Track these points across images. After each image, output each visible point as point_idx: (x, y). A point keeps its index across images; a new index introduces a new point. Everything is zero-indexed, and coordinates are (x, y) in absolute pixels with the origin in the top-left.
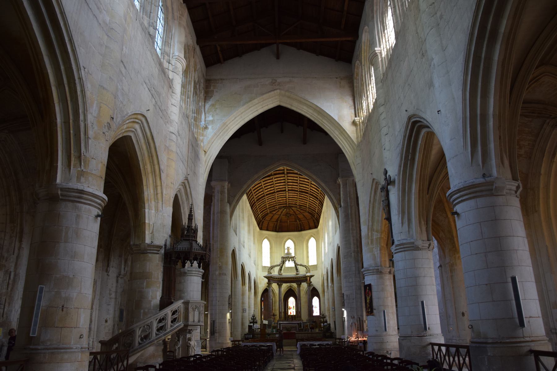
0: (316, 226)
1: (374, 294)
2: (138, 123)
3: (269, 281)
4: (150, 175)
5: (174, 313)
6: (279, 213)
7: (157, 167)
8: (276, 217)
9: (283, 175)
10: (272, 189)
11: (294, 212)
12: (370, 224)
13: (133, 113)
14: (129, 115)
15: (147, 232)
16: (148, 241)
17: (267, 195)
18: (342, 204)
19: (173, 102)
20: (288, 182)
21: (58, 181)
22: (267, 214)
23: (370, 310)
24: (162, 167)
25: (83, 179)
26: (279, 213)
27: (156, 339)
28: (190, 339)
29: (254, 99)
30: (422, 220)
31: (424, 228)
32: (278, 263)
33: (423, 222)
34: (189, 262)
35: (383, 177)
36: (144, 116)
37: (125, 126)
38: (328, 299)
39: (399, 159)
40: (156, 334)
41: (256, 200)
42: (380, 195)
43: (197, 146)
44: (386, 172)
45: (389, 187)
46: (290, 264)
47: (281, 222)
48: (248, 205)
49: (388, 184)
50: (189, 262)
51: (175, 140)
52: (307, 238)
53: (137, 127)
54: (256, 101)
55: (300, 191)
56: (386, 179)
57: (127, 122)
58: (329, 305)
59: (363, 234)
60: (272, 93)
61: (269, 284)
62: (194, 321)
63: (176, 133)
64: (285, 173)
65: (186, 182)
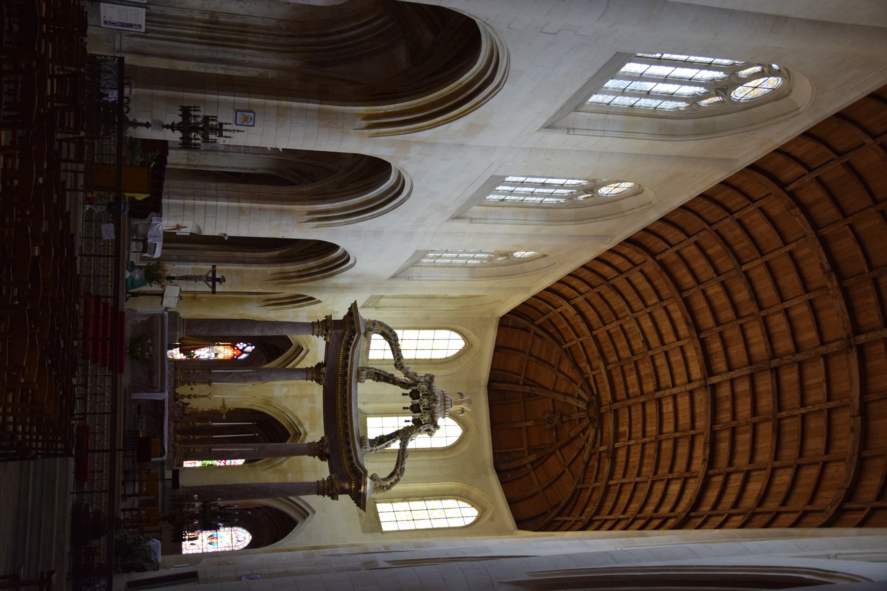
8: (546, 377)
11: (572, 440)
52: (475, 492)
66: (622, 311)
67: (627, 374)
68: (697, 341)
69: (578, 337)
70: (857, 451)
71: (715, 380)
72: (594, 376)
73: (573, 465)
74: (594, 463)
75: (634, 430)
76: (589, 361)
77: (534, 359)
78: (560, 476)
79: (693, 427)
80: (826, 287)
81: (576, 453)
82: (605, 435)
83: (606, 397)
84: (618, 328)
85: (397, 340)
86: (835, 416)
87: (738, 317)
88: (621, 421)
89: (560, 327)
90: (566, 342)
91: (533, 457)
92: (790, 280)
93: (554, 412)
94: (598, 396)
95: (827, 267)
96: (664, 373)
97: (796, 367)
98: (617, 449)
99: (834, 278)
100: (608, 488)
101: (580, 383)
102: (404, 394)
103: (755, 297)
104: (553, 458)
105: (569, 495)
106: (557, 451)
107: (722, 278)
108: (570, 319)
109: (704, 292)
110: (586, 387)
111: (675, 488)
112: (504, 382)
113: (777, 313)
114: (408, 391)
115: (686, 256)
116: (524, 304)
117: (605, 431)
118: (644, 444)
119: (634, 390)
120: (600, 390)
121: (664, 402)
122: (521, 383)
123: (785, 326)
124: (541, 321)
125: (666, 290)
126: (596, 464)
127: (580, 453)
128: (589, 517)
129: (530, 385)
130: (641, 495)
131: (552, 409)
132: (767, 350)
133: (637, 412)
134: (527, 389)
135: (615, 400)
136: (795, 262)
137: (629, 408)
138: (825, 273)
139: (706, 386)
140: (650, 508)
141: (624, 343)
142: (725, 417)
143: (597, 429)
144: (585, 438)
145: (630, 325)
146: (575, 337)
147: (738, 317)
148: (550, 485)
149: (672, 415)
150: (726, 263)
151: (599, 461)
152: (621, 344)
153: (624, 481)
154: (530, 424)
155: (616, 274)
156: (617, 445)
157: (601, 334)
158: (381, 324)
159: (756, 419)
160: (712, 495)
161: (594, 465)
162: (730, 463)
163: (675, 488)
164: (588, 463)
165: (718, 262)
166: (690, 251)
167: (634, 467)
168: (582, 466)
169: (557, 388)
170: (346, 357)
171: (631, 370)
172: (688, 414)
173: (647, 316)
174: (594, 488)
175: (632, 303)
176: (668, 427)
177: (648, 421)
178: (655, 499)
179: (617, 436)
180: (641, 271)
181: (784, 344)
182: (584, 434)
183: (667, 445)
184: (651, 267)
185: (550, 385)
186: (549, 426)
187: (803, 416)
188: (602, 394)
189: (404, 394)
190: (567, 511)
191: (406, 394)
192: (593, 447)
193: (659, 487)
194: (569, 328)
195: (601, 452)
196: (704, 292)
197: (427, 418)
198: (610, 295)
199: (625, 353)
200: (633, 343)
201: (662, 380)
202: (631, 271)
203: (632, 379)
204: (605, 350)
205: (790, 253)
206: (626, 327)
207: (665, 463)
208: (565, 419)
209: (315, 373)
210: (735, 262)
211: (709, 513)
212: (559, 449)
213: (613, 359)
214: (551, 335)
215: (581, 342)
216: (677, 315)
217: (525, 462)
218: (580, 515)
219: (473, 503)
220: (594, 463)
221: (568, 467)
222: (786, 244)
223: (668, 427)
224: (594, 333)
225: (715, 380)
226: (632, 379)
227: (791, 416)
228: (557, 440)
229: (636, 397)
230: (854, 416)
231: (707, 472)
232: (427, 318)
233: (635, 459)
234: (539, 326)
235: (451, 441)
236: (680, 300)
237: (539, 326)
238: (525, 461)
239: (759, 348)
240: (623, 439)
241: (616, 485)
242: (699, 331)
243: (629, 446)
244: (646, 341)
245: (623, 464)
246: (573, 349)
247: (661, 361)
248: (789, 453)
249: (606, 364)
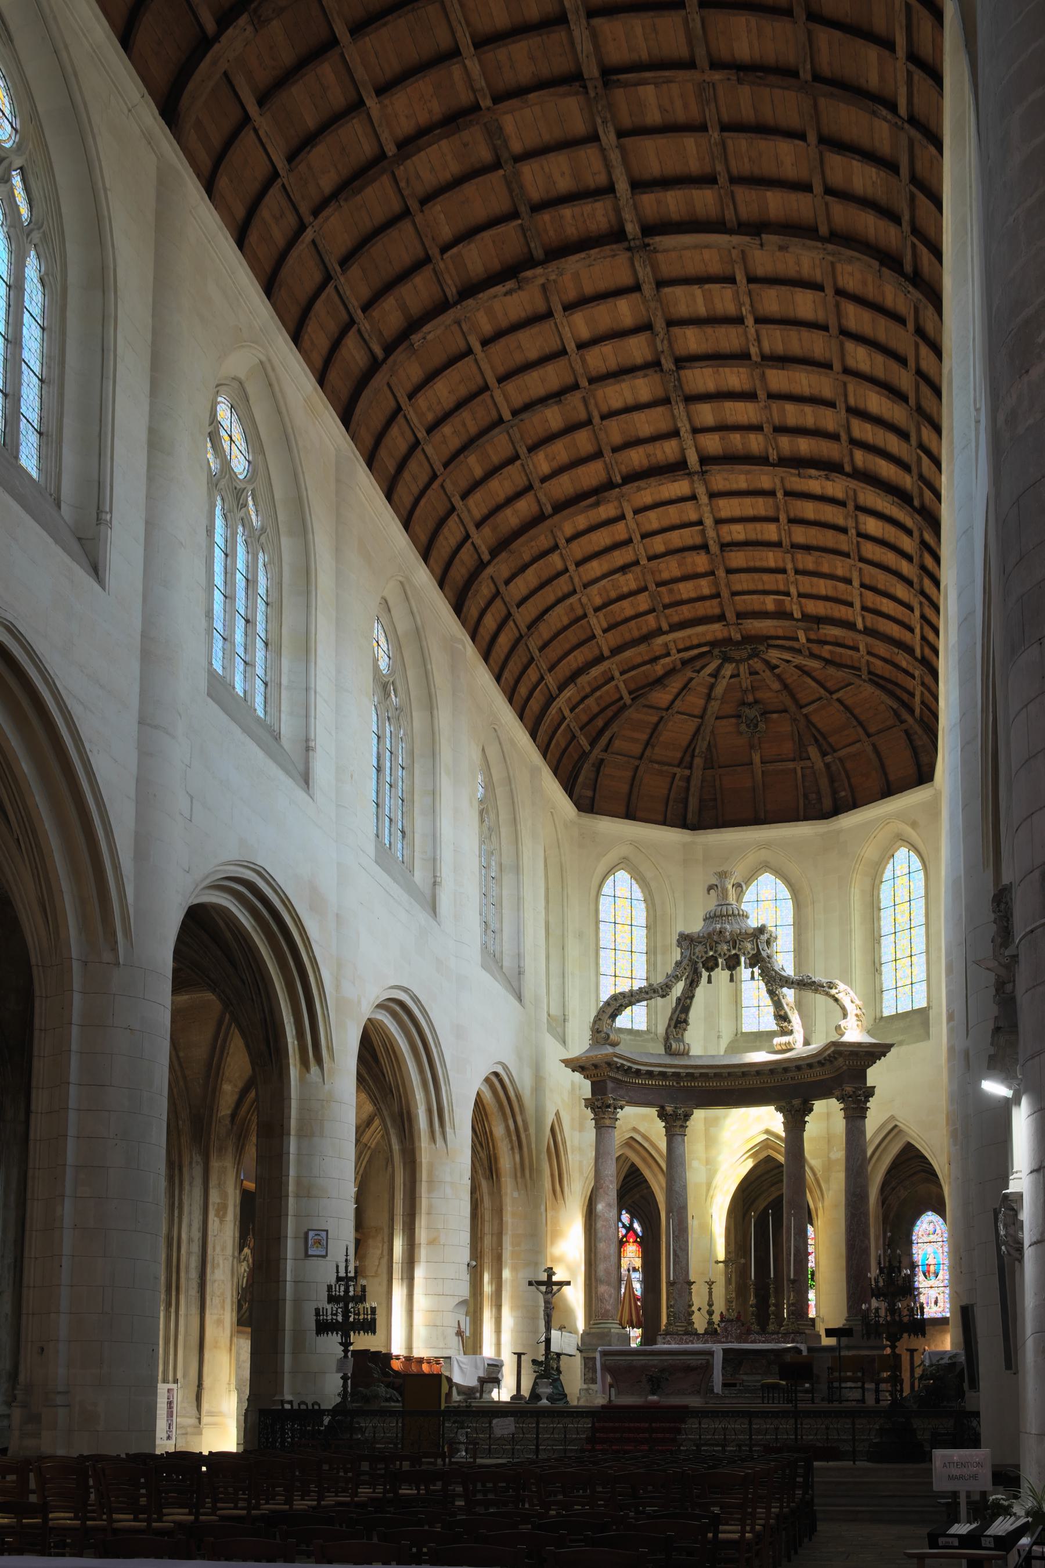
6: (694, 701)
8: (678, 730)
11: (785, 686)
26: (694, 701)
47: (710, 764)
66: (572, 609)
67: (678, 598)
68: (626, 489)
69: (612, 678)
70: (819, 244)
71: (693, 459)
72: (679, 651)
73: (829, 685)
74: (826, 651)
75: (774, 587)
76: (655, 660)
77: (648, 753)
78: (846, 707)
79: (772, 493)
80: (543, 286)
81: (809, 680)
82: (780, 632)
83: (715, 631)
84: (600, 614)
85: (623, 994)
86: (760, 272)
87: (589, 422)
88: (757, 607)
89: (596, 709)
90: (621, 698)
91: (813, 751)
92: (531, 343)
93: (739, 716)
94: (713, 644)
95: (510, 285)
96: (676, 538)
97: (676, 330)
98: (803, 615)
99: (529, 273)
100: (869, 632)
101: (690, 674)
102: (709, 981)
103: (557, 396)
104: (815, 719)
105: (878, 692)
106: (805, 711)
107: (523, 451)
108: (583, 694)
109: (544, 480)
110: (698, 664)
111: (872, 526)
112: (685, 802)
113: (584, 361)
114: (705, 974)
115: (485, 511)
116: (556, 773)
117: (772, 632)
118: (797, 572)
119: (705, 586)
120: (703, 641)
121: (727, 539)
122: (687, 772)
123: (607, 349)
124: (584, 742)
125: (540, 538)
126: (827, 647)
127: (808, 674)
128: (917, 664)
129: (693, 756)
130: (882, 580)
131: (733, 720)
132: (645, 376)
133: (742, 582)
134: (698, 762)
135: (721, 618)
136: (499, 334)
137: (734, 594)
138: (520, 288)
139: (703, 473)
140: (905, 567)
141: (625, 603)
142: (755, 443)
143: (769, 646)
144: (783, 665)
145: (595, 595)
146: (613, 683)
147: (589, 422)
148: (861, 724)
149: (750, 526)
150: (498, 446)
151: (826, 643)
152: (627, 608)
153: (857, 605)
154: (757, 758)
155: (511, 623)
156: (797, 615)
157: (605, 642)
158: (598, 1019)
159: (762, 395)
160: (886, 470)
161: (831, 652)
162: (835, 437)
163: (872, 526)
164: (828, 662)
165: (496, 460)
166: (478, 505)
167: (835, 588)
168: (831, 670)
169: (697, 711)
170: (650, 1074)
171: (671, 591)
172: (748, 501)
173: (581, 569)
174: (869, 653)
175: (560, 594)
176: (770, 532)
177: (758, 564)
178: (890, 558)
179: (782, 614)
180: (507, 582)
181: (637, 349)
182: (777, 667)
183: (800, 535)
184: (501, 568)
185: (691, 725)
186: (762, 726)
187: (758, 321)
188: (709, 638)
189: (709, 981)
190: (905, 697)
191: (709, 977)
192: (799, 651)
193: (870, 550)
194: (598, 693)
195: (809, 640)
196: (544, 480)
197: (749, 946)
198: (545, 630)
199: (643, 602)
200: (625, 590)
201: (690, 542)
202: (507, 599)
203: (686, 590)
204: (636, 634)
205: (485, 343)
206: (598, 601)
207: (829, 538)
208: (750, 699)
209: (676, 1124)
210: (497, 430)
211: (916, 477)
212: (802, 707)
213: (651, 621)
214: (607, 725)
215: (622, 674)
216: (582, 521)
217: (822, 765)
218: (913, 677)
220: (826, 651)
221: (831, 693)
222: (469, 352)
223: (770, 532)
224: (606, 653)
225: (693, 459)
226: (686, 590)
227: (758, 339)
228: (785, 711)
229: (716, 584)
230: (762, 245)
231: (848, 475)
232: (580, 935)
233: (823, 587)
234: (593, 744)
236: (557, 518)
237: (593, 744)
238: (819, 765)
239: (643, 388)
240: (787, 603)
241: (863, 618)
242: (609, 485)
243: (800, 595)
244: (624, 569)
245: (829, 604)
246: (633, 686)
247: (658, 544)
248: (817, 345)
249: (659, 632)
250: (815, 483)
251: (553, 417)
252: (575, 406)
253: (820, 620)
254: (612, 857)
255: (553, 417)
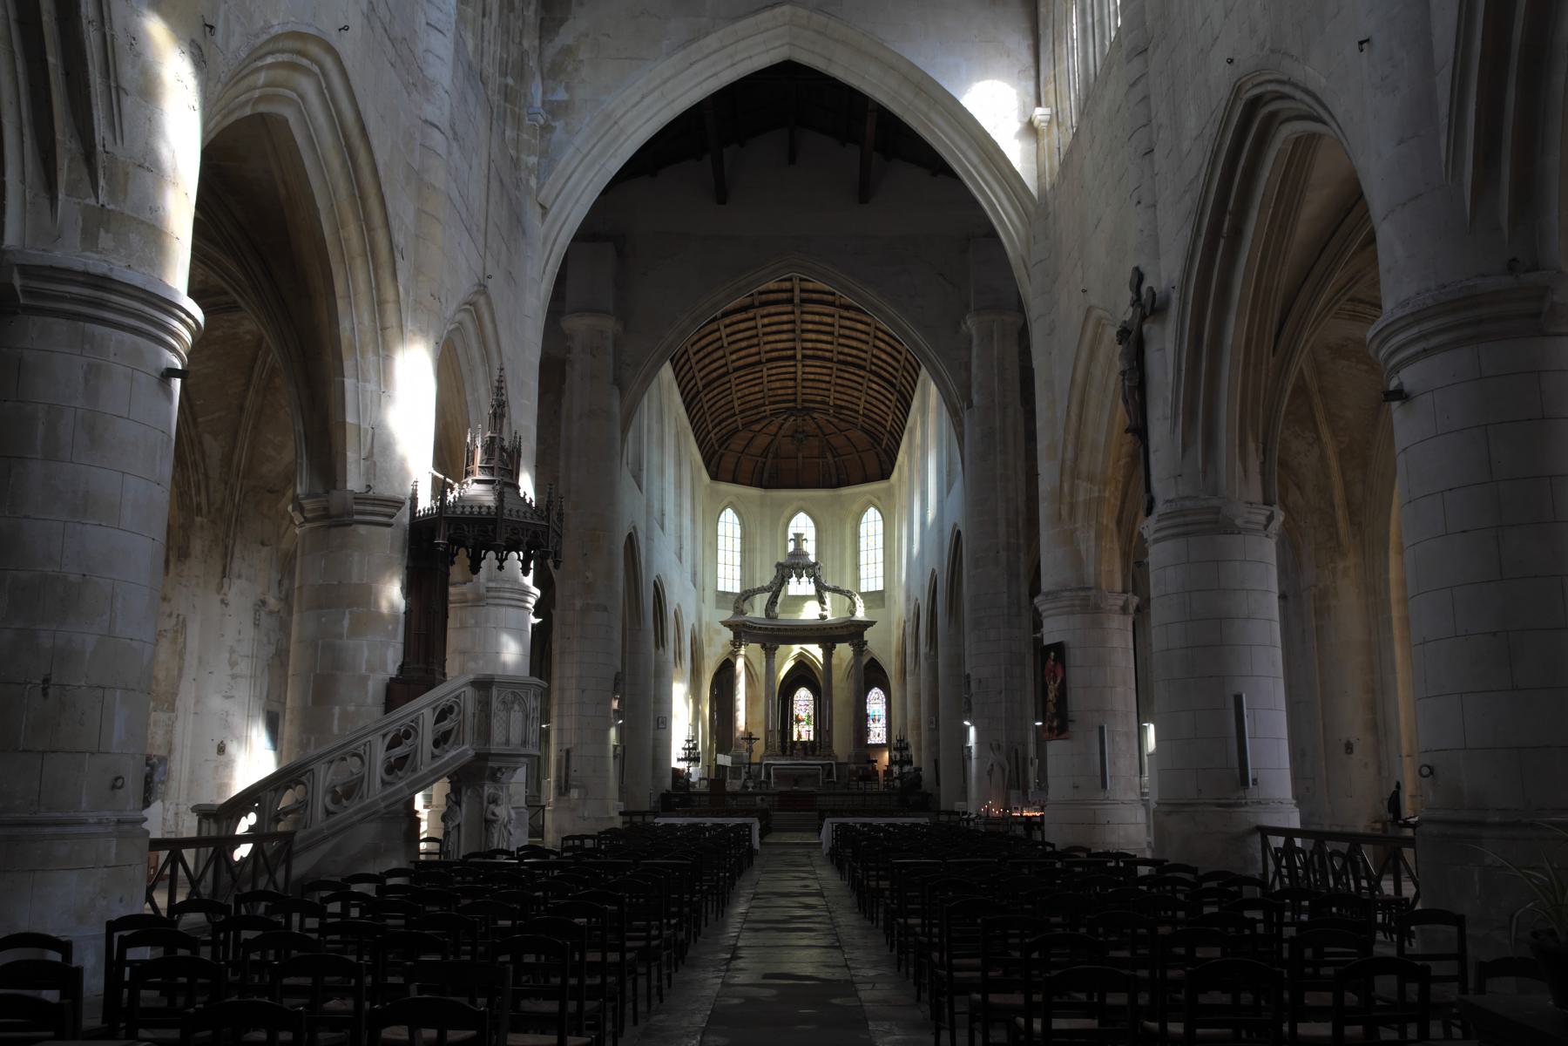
0: (885, 474)
1: (1075, 676)
2: (307, 72)
3: (737, 636)
4: (359, 262)
5: (443, 715)
7: (380, 236)
9: (789, 308)
10: (753, 350)
12: (1070, 455)
13: (289, 28)
14: (273, 32)
15: (351, 455)
16: (354, 482)
17: (736, 370)
18: (975, 398)
19: (435, 16)
20: (803, 331)
21: (11, 239)
22: (736, 430)
23: (1060, 722)
24: (399, 239)
25: (105, 240)
26: (773, 429)
27: (384, 798)
28: (494, 800)
29: (707, 34)
30: (1250, 438)
31: (1254, 464)
32: (767, 583)
33: (1251, 446)
34: (491, 554)
35: (1128, 295)
36: (330, 49)
37: (262, 78)
38: (918, 695)
39: (1188, 232)
40: (384, 783)
41: (700, 385)
42: (1111, 357)
43: (518, 187)
44: (1139, 276)
45: (1145, 327)
46: (800, 586)
48: (678, 399)
49: (1143, 318)
50: (491, 554)
51: (442, 150)
53: (307, 86)
54: (712, 41)
55: (839, 362)
56: (1137, 301)
57: (269, 60)
58: (918, 713)
59: (1045, 484)
60: (767, 15)
61: (737, 642)
62: (507, 742)
63: (445, 126)
64: (797, 300)
65: (482, 301)
71: (799, 356)
91: (829, 456)
150: (720, 353)
185: (769, 438)
219: (864, 510)
235: (811, 523)
250: (852, 369)
251: (744, 344)
252: (755, 341)
253: (842, 407)
254: (726, 502)
255: (744, 344)
